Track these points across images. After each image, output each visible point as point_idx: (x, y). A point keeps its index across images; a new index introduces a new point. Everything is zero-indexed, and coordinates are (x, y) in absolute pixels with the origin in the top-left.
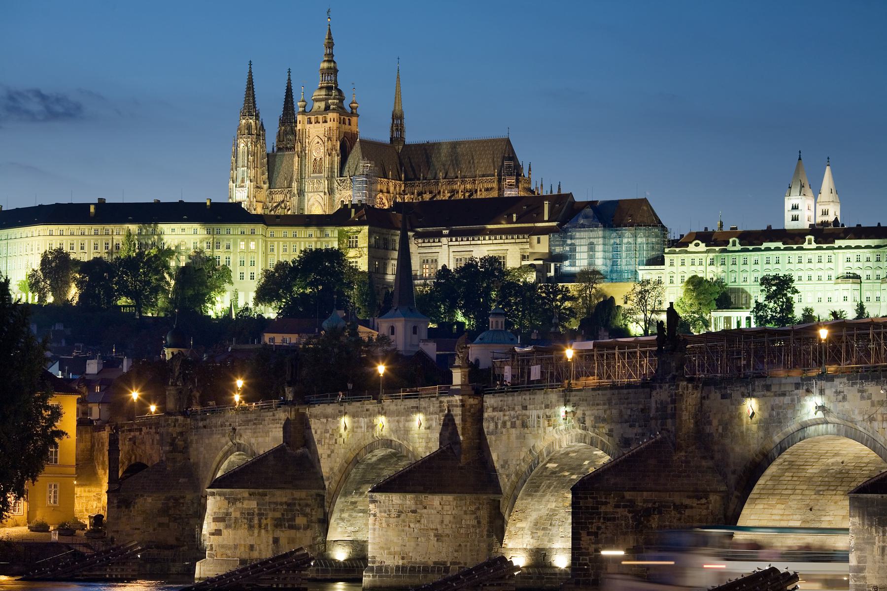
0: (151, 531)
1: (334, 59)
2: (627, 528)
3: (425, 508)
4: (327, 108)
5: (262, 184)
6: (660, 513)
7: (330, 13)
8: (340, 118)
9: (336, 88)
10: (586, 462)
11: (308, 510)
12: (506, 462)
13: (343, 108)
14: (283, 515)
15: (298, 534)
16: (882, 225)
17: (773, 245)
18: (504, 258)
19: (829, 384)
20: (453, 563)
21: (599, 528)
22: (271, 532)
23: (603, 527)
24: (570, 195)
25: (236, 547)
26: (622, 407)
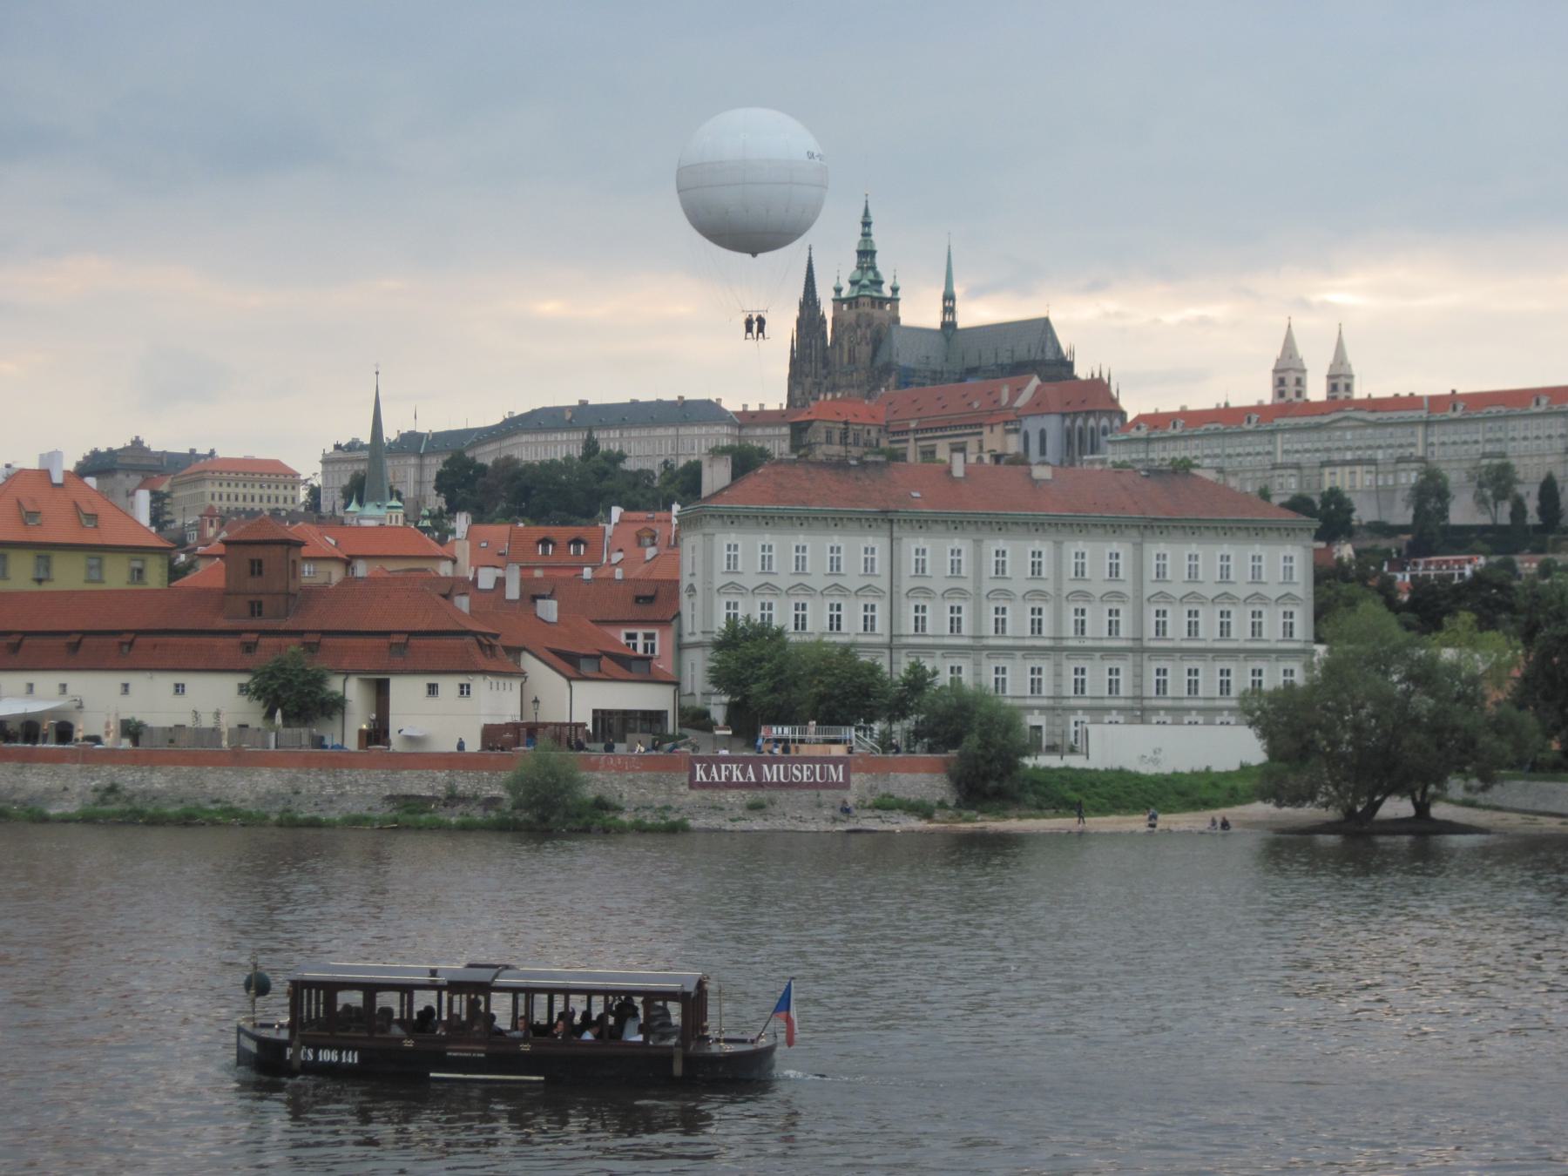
1: (873, 238)
4: (859, 291)
9: (873, 268)
13: (879, 291)
17: (1212, 427)
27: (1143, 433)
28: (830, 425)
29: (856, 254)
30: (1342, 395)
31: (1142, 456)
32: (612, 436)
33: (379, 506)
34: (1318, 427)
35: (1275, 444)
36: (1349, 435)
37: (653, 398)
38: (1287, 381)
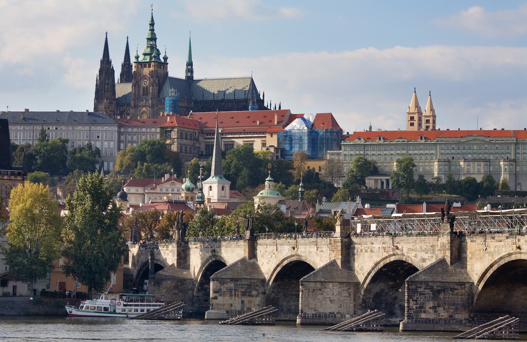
0: (170, 296)
1: (155, 32)
2: (430, 298)
3: (325, 288)
4: (151, 58)
5: (113, 101)
6: (444, 291)
7: (152, 6)
8: (158, 65)
9: (156, 47)
10: (399, 268)
11: (257, 288)
12: (362, 268)
13: (159, 59)
14: (246, 290)
15: (253, 299)
16: (461, 130)
18: (252, 144)
19: (522, 237)
20: (337, 313)
21: (417, 298)
22: (240, 298)
23: (419, 297)
24: (288, 111)
25: (224, 305)
26: (422, 245)
27: (362, 142)
28: (182, 129)
29: (146, 40)
30: (431, 125)
31: (362, 152)
32: (51, 129)
33: (221, 177)
34: (459, 143)
35: (436, 149)
36: (475, 147)
37: (69, 110)
38: (415, 119)
